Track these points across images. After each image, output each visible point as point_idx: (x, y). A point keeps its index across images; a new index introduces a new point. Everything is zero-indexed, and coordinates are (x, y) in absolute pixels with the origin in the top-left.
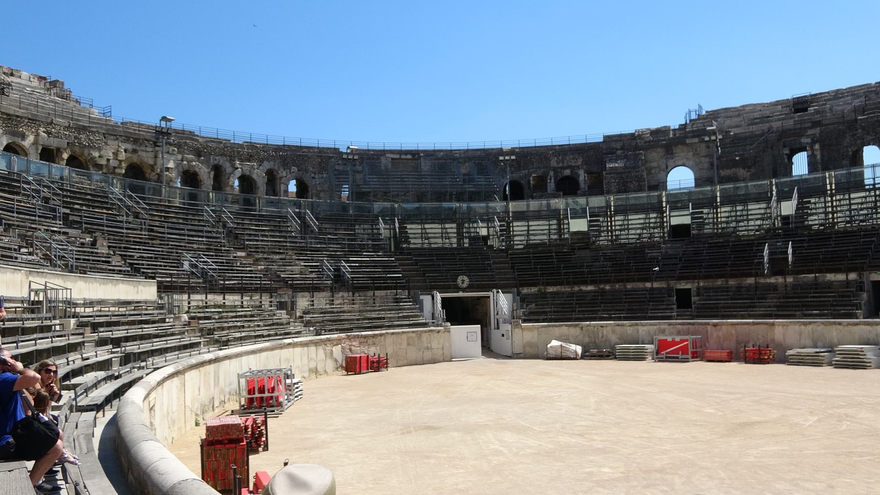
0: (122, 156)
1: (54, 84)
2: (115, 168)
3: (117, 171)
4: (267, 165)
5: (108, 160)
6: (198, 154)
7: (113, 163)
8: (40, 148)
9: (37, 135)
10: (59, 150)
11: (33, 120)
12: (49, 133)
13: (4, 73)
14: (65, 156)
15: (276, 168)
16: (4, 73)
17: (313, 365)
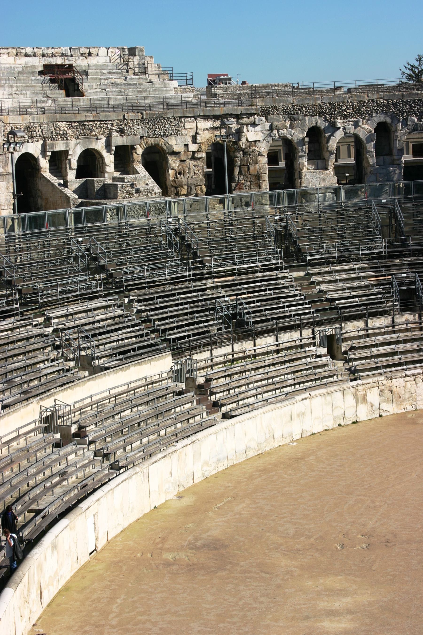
0: (202, 138)
1: (132, 52)
2: (194, 153)
3: (197, 155)
4: (378, 118)
5: (187, 146)
6: (291, 115)
7: (193, 148)
8: (114, 148)
9: (109, 137)
10: (133, 147)
11: (105, 121)
12: (121, 132)
13: (82, 55)
14: (140, 151)
15: (389, 120)
16: (82, 55)
17: (339, 412)
